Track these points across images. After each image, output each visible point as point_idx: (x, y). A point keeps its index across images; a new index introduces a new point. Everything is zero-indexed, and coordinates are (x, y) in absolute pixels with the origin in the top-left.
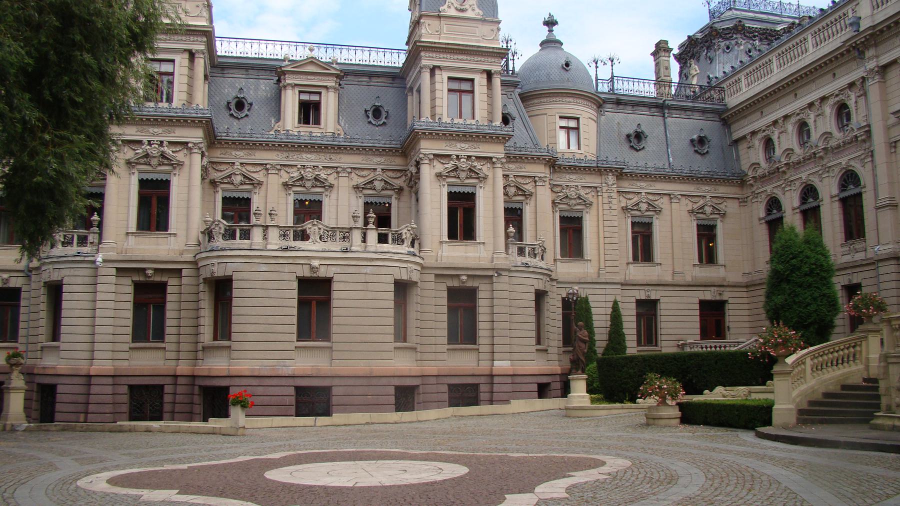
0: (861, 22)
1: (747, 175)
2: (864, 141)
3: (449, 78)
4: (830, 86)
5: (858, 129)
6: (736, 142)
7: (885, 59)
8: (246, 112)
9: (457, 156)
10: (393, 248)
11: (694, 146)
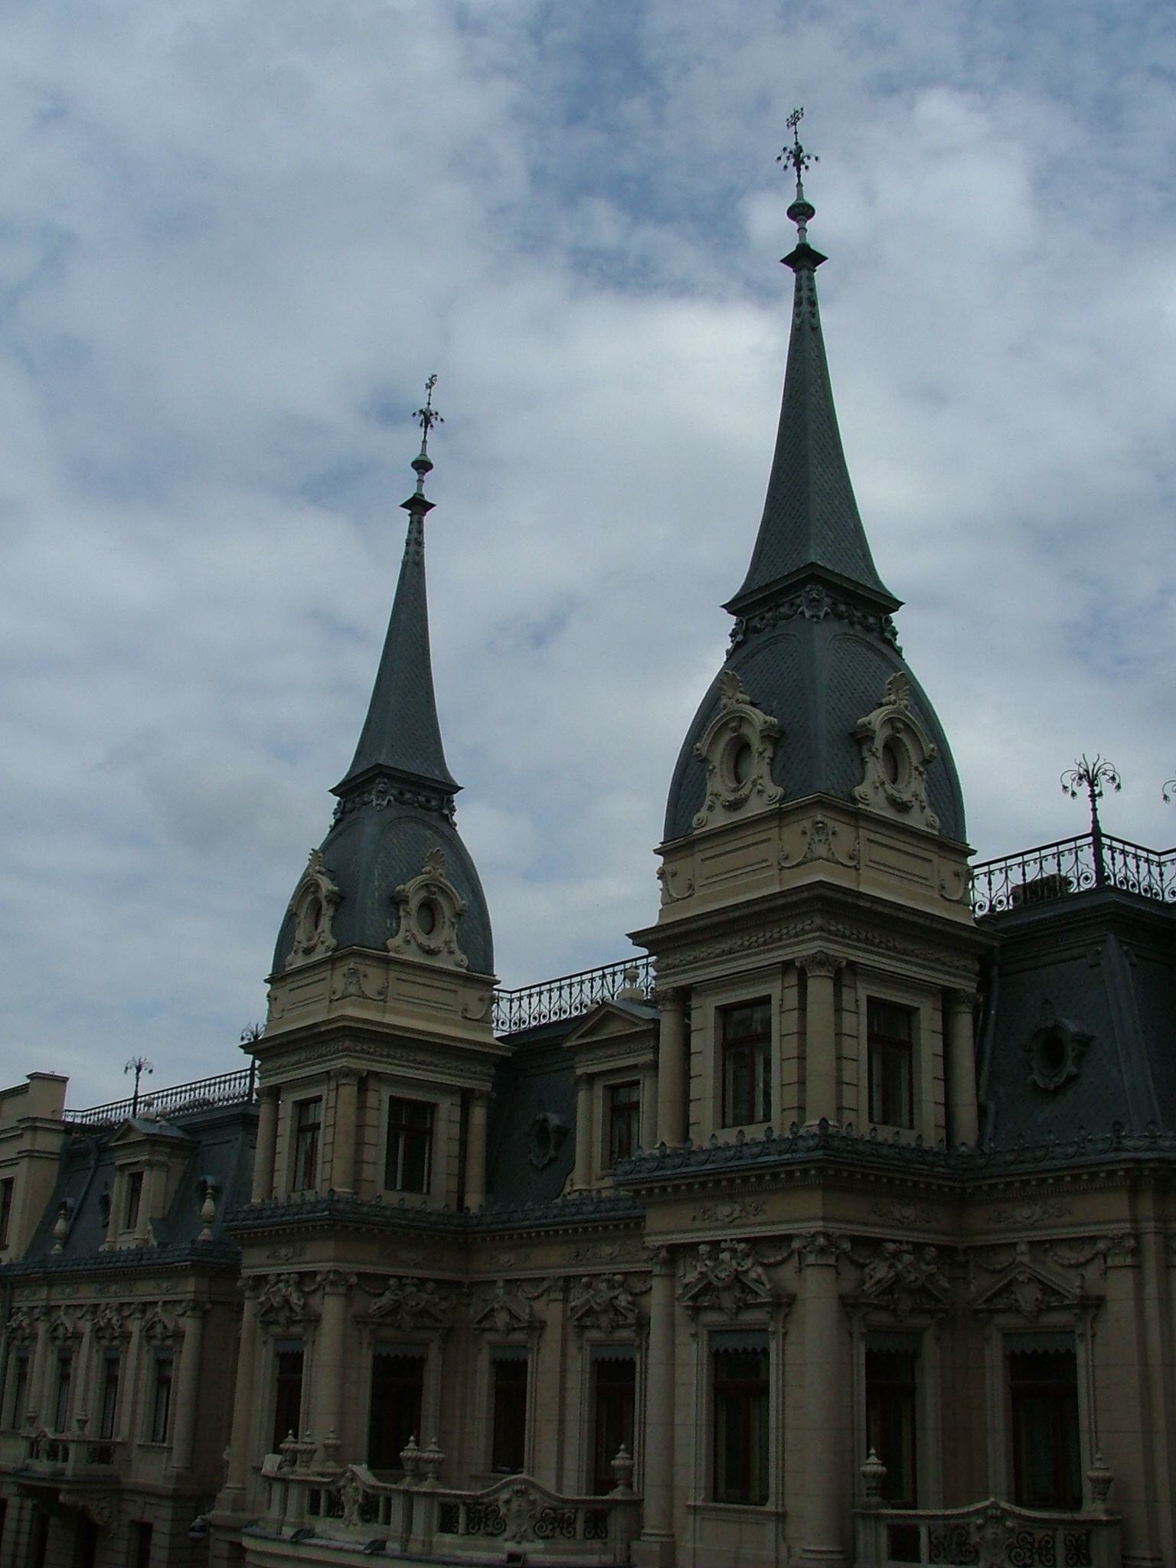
3: (724, 1011)
8: (552, 1153)
9: (715, 1245)
10: (461, 1547)
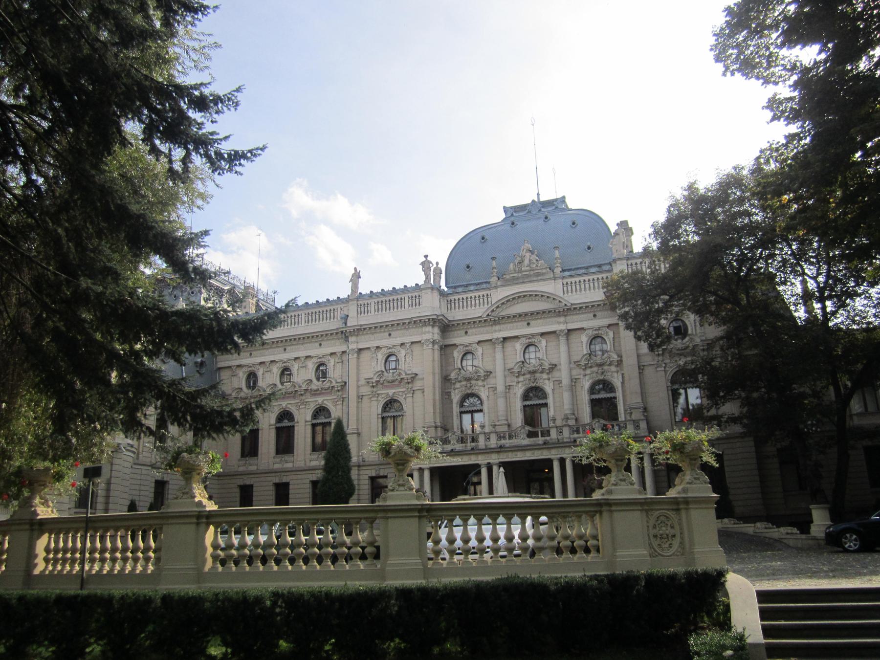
0: (349, 320)
1: (231, 395)
2: (338, 391)
4: (314, 350)
5: (337, 383)
6: (220, 369)
7: (361, 346)
11: (197, 366)
